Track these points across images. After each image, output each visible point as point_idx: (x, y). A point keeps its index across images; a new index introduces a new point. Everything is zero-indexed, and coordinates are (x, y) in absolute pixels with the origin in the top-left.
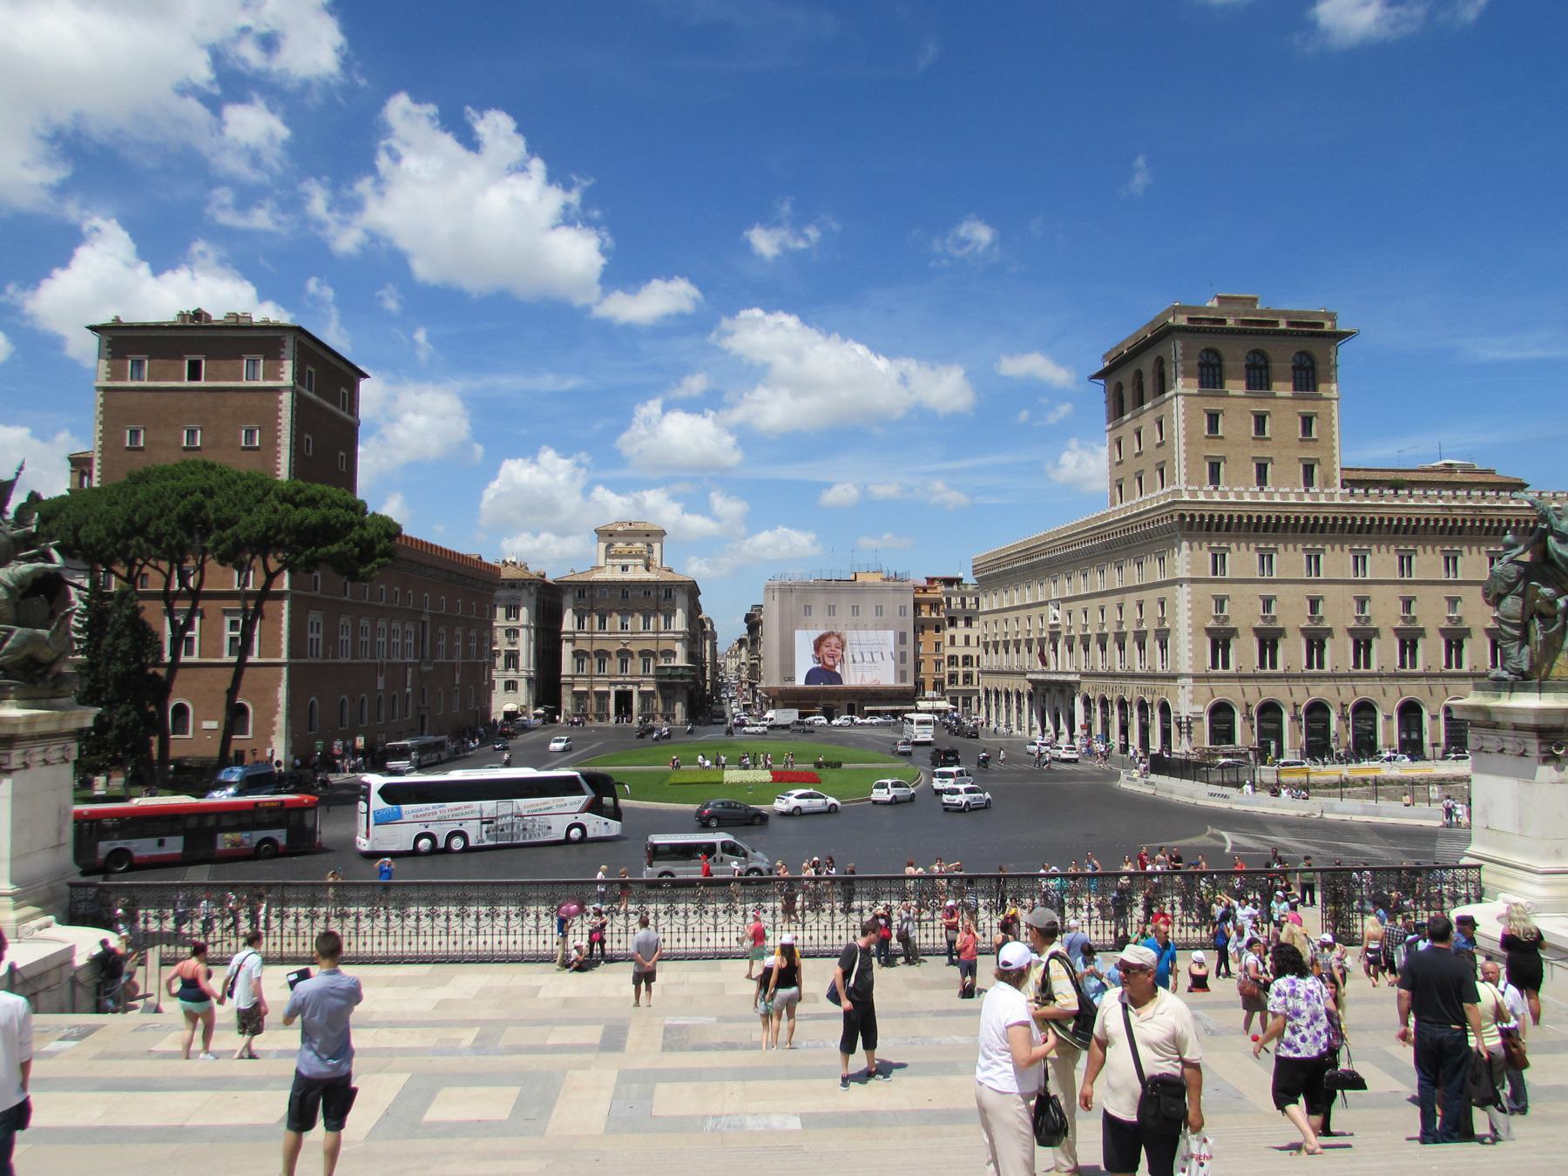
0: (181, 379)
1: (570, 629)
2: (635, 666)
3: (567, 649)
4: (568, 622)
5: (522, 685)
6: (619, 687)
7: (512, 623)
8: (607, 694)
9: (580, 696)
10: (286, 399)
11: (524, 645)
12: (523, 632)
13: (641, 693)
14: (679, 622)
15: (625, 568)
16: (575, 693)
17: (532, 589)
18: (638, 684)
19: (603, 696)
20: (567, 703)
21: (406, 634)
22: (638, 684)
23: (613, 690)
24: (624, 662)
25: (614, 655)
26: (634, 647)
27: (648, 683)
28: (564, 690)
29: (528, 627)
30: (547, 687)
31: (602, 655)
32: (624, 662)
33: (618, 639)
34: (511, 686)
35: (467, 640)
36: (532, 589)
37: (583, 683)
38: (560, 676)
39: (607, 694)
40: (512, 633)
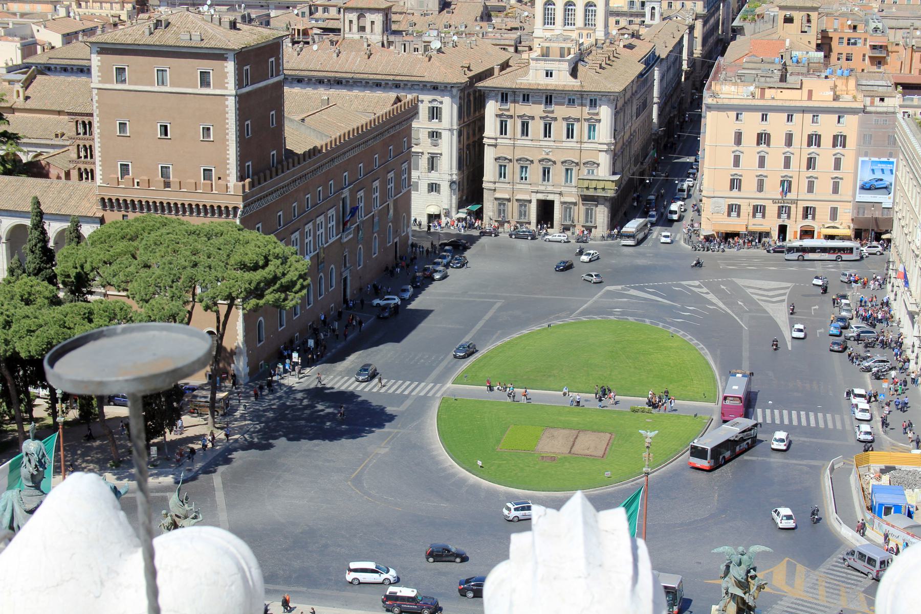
0: (152, 85)
1: (493, 135)
2: (557, 173)
3: (489, 155)
4: (491, 127)
5: (445, 188)
6: (541, 197)
7: (435, 125)
8: (530, 201)
9: (502, 202)
10: (231, 103)
11: (449, 149)
12: (446, 135)
13: (563, 203)
14: (604, 132)
15: (549, 74)
16: (496, 199)
17: (455, 91)
18: (561, 194)
19: (524, 203)
20: (489, 208)
21: (328, 220)
22: (561, 194)
23: (535, 198)
24: (546, 172)
25: (536, 162)
26: (558, 157)
27: (570, 194)
28: (486, 195)
29: (451, 130)
30: (471, 189)
31: (524, 164)
32: (546, 172)
33: (541, 147)
34: (433, 188)
35: (385, 183)
36: (455, 91)
37: (503, 190)
38: (482, 182)
39: (530, 201)
40: (435, 135)
